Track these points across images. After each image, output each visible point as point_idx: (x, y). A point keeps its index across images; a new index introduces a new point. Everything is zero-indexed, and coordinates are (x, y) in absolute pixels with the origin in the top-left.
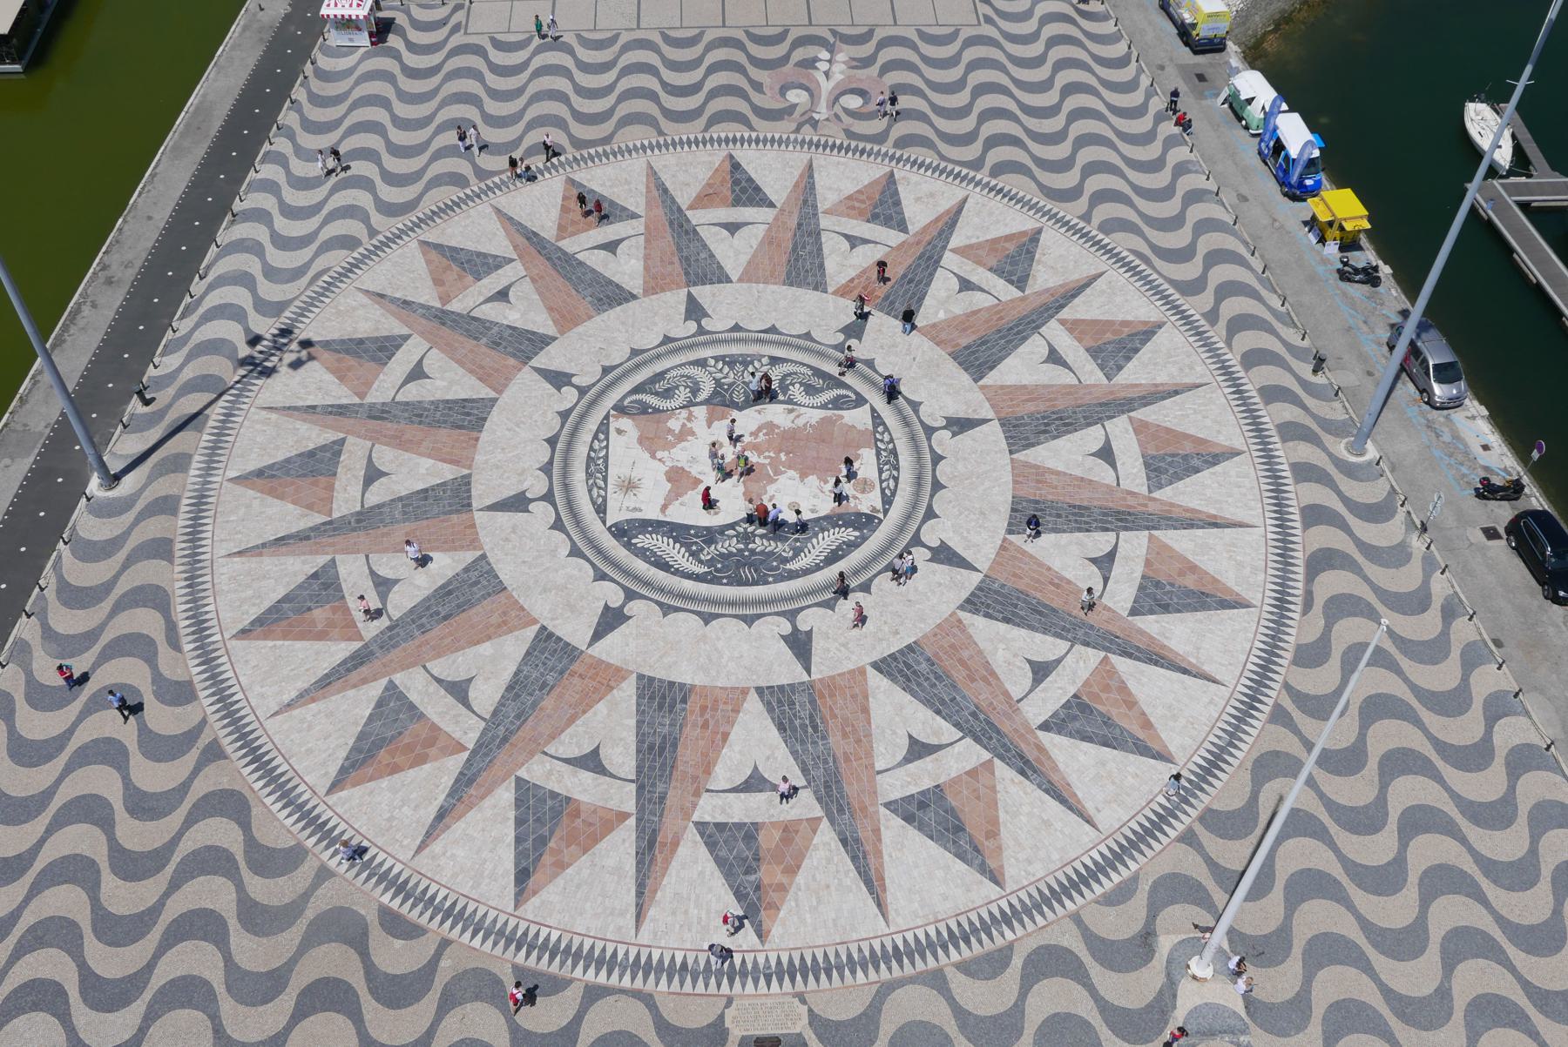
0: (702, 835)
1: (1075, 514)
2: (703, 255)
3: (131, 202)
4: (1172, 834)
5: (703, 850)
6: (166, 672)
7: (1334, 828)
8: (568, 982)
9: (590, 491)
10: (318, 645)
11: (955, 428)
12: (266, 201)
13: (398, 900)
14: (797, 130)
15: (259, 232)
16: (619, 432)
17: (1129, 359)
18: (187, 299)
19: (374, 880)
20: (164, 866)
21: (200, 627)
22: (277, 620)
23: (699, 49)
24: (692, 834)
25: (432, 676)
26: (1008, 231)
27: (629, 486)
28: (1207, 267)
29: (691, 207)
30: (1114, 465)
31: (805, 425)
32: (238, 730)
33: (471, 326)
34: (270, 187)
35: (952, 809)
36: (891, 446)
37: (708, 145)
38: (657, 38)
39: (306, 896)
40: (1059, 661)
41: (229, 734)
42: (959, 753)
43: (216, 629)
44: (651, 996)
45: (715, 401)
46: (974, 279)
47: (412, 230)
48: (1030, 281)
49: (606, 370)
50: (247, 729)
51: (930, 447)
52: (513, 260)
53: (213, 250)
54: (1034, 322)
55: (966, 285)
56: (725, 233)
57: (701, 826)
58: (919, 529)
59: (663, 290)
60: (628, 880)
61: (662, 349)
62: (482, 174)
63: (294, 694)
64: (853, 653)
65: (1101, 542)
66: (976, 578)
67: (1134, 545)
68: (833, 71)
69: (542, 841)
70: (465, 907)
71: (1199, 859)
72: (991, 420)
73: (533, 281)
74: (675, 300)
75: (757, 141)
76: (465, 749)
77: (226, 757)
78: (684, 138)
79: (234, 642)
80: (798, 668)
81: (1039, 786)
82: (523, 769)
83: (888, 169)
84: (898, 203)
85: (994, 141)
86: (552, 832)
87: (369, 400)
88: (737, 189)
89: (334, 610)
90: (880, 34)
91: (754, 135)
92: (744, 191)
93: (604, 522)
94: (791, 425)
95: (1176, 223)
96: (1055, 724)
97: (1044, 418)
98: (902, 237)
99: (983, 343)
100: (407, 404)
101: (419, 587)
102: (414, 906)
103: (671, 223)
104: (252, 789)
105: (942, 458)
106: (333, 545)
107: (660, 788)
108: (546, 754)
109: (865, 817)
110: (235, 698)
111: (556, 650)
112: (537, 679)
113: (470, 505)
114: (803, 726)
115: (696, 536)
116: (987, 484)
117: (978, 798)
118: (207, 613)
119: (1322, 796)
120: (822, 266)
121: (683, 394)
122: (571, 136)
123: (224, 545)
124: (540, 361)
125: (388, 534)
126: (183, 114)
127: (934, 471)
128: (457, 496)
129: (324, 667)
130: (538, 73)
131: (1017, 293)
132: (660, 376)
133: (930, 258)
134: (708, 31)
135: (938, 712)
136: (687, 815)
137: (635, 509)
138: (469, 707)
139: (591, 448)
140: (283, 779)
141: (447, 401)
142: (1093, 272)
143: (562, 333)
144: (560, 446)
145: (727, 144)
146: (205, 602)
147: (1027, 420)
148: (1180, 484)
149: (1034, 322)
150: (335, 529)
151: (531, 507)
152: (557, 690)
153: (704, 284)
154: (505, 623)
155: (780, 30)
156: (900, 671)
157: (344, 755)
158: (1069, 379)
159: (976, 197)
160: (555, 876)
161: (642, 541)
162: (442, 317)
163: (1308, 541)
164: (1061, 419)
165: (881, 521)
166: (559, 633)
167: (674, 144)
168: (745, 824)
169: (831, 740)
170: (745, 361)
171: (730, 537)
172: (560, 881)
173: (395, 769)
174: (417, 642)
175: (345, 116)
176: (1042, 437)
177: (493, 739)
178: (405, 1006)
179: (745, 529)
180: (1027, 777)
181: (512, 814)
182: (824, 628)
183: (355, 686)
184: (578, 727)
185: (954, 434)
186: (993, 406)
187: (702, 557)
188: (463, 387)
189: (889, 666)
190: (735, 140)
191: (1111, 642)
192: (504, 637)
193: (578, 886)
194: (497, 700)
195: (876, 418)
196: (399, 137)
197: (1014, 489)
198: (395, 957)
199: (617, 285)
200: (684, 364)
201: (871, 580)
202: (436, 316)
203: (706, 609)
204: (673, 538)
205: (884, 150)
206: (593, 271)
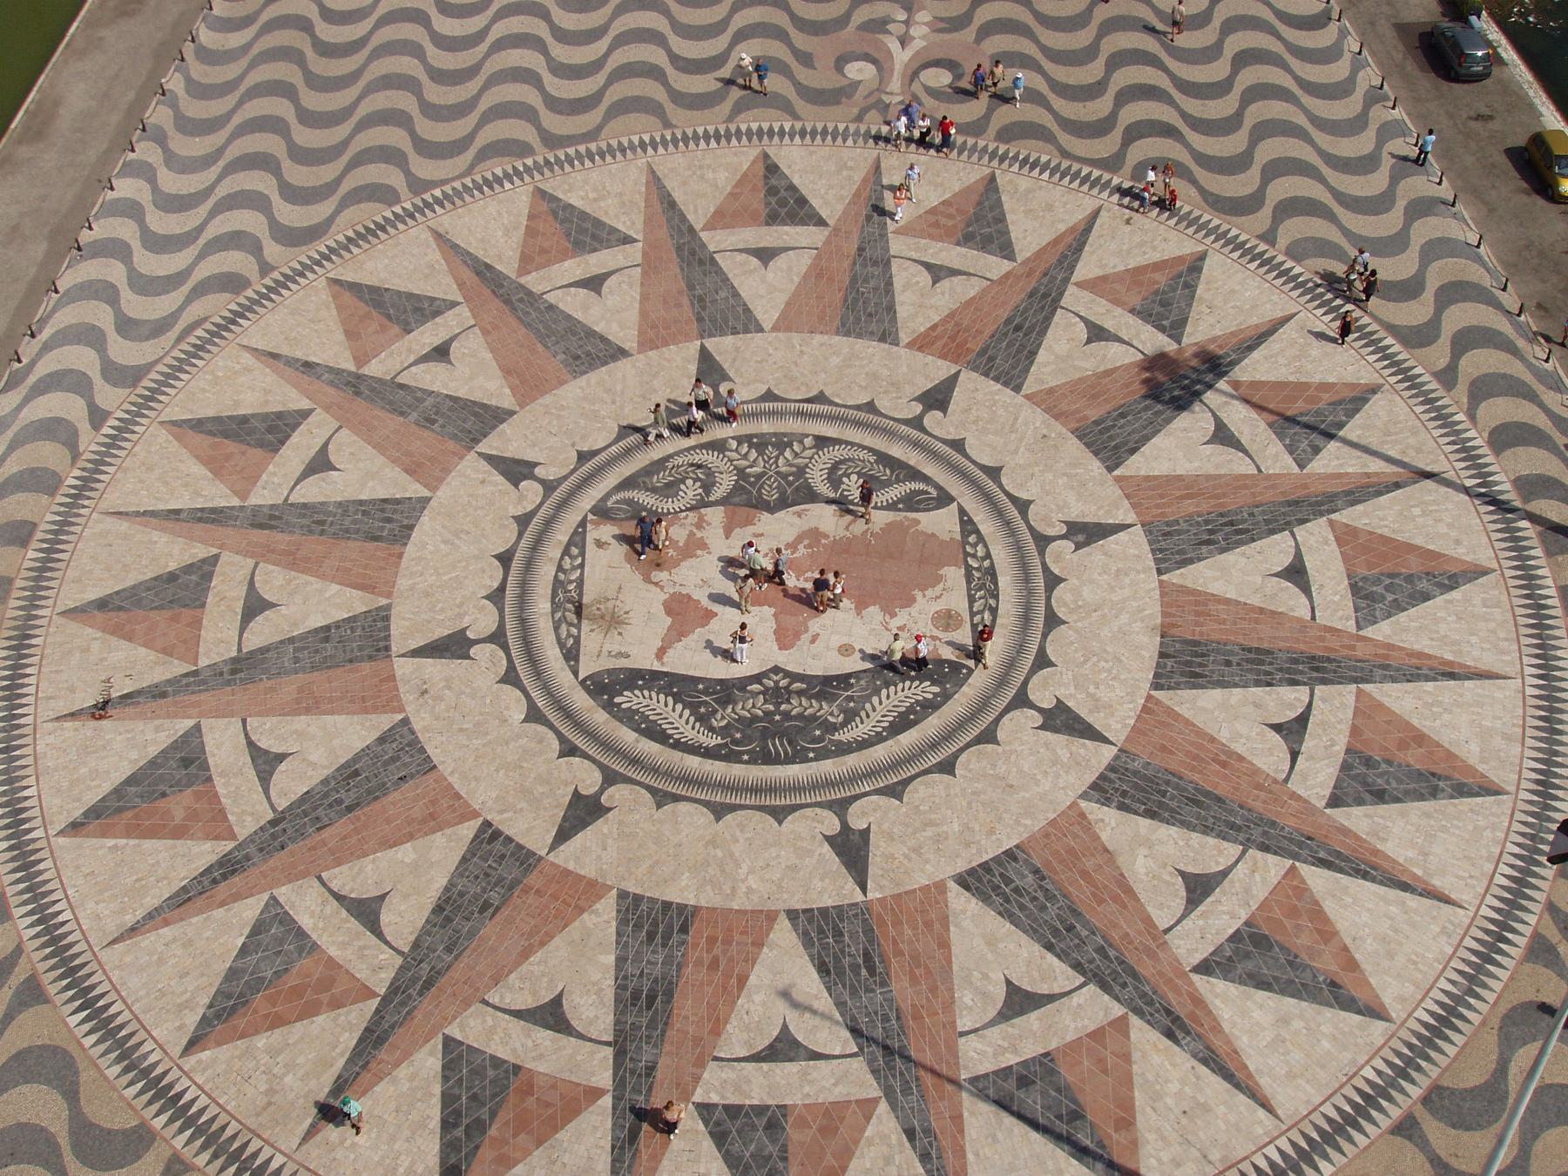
1: (1247, 661)
2: (723, 294)
4: (1385, 1123)
5: (708, 1144)
9: (556, 629)
11: (1081, 538)
12: (125, 230)
14: (859, 118)
15: (115, 272)
16: (600, 544)
22: (119, 810)
25: (331, 891)
26: (1156, 257)
28: (1440, 306)
29: (709, 226)
30: (1306, 589)
32: (63, 962)
34: (132, 210)
35: (1068, 1088)
36: (987, 563)
37: (734, 141)
40: (1225, 873)
45: (736, 500)
46: (1108, 324)
47: (319, 264)
48: (1188, 329)
49: (583, 457)
50: (77, 962)
51: (1044, 565)
52: (458, 304)
55: (1097, 334)
56: (754, 262)
57: (705, 1109)
59: (666, 344)
62: (418, 186)
63: (140, 914)
64: (927, 861)
65: (1287, 700)
66: (1107, 753)
69: (479, 1127)
71: (1421, 1158)
72: (1130, 526)
73: (485, 332)
75: (803, 133)
76: (374, 995)
77: (47, 1001)
78: (700, 131)
79: (61, 840)
80: (850, 885)
81: (1195, 1056)
83: (988, 171)
84: (1001, 219)
85: (1134, 133)
86: (493, 1115)
87: (254, 500)
88: (773, 200)
89: (198, 796)
91: (798, 125)
92: (783, 203)
96: (1218, 963)
97: (1207, 522)
98: (1006, 266)
99: (1122, 416)
100: (305, 506)
101: (313, 765)
103: (679, 248)
104: (81, 1045)
108: (487, 1004)
109: (941, 1098)
110: (61, 918)
112: (476, 897)
113: (387, 648)
114: (855, 968)
115: (705, 692)
116: (1124, 618)
117: (1105, 1071)
118: (26, 798)
120: (891, 309)
121: (691, 491)
123: (52, 703)
124: (489, 445)
125: (272, 689)
127: (1048, 599)
129: (182, 874)
130: (499, 45)
132: (660, 464)
133: (1045, 296)
135: (1049, 947)
137: (620, 655)
138: (379, 935)
139: (560, 568)
140: (123, 1033)
141: (361, 503)
142: (1279, 314)
143: (522, 406)
144: (517, 564)
145: (760, 139)
147: (1184, 526)
148: (1402, 617)
150: (203, 682)
151: (472, 652)
154: (432, 816)
156: (996, 888)
157: (207, 1001)
158: (1243, 466)
161: (627, 700)
162: (355, 384)
164: (1231, 523)
165: (971, 671)
166: (508, 832)
167: (685, 139)
168: (768, 1107)
169: (894, 986)
170: (782, 442)
171: (755, 694)
173: (277, 1022)
174: (308, 842)
175: (233, 111)
176: (1204, 549)
177: (414, 980)
179: (776, 683)
180: (1176, 1041)
181: (437, 1089)
182: (885, 826)
183: (222, 904)
184: (534, 963)
185: (1078, 547)
186: (1134, 506)
187: (715, 723)
188: (387, 481)
189: (980, 880)
191: (1300, 845)
192: (433, 837)
195: (968, 525)
196: (305, 137)
199: (603, 339)
200: (693, 448)
201: (956, 756)
202: (348, 384)
204: (674, 695)
205: (981, 144)
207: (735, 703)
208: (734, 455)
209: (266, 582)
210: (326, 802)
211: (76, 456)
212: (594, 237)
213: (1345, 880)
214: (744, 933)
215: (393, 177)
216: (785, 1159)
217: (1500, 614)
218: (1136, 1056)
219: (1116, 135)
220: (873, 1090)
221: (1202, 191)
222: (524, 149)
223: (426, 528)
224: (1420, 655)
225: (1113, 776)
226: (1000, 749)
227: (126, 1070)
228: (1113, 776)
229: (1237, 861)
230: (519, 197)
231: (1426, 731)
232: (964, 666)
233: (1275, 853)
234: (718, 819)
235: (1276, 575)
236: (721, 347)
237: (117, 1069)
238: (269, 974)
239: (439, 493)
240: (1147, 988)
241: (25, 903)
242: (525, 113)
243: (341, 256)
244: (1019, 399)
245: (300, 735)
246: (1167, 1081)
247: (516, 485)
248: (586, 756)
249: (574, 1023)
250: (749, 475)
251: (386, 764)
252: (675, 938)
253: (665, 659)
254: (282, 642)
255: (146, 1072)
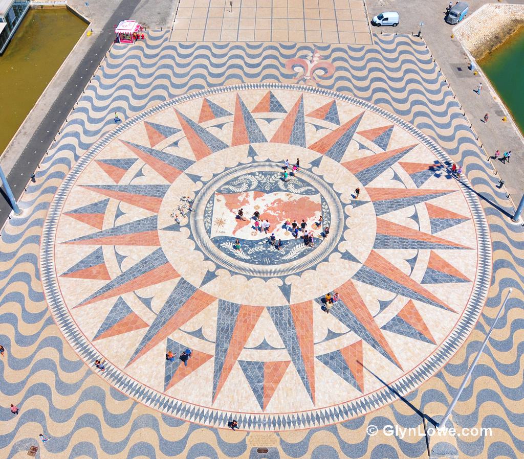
0: (241, 366)
1: (402, 242)
3: (36, 104)
5: (241, 372)
6: (34, 289)
7: (498, 373)
8: (185, 421)
9: (205, 224)
10: (95, 281)
11: (355, 205)
12: (87, 105)
13: (118, 385)
14: (298, 83)
16: (218, 200)
17: (426, 179)
18: (53, 142)
19: (109, 376)
20: (28, 365)
21: (48, 270)
23: (260, 50)
24: (237, 366)
26: (380, 126)
27: (221, 222)
28: (459, 144)
29: (254, 111)
30: (418, 222)
31: (294, 201)
32: (60, 313)
33: (161, 155)
34: (89, 99)
36: (328, 211)
37: (262, 88)
38: (245, 47)
39: (82, 381)
40: (391, 301)
41: (57, 314)
42: (349, 337)
43: (54, 273)
44: (216, 429)
46: (366, 145)
47: (142, 117)
48: (388, 146)
49: (215, 176)
53: (65, 123)
54: (389, 163)
55: (362, 147)
57: (241, 362)
58: (337, 245)
59: (240, 144)
60: (210, 382)
61: (237, 168)
62: (171, 96)
65: (411, 253)
66: (359, 266)
67: (424, 256)
68: (314, 60)
70: (144, 390)
71: (443, 384)
73: (188, 138)
74: (245, 148)
75: (281, 87)
76: (148, 326)
78: (252, 84)
79: (60, 278)
80: (285, 300)
81: (380, 352)
82: (171, 335)
84: (336, 113)
85: (376, 90)
87: (120, 184)
88: (272, 105)
89: (100, 267)
90: (332, 47)
91: (280, 85)
92: (275, 106)
93: (210, 237)
94: (288, 200)
95: (447, 126)
97: (390, 202)
98: (337, 126)
99: (368, 171)
101: (133, 260)
102: (124, 387)
103: (245, 117)
105: (348, 216)
106: (101, 241)
107: (225, 345)
108: (180, 330)
110: (59, 300)
111: (187, 288)
113: (156, 227)
114: (285, 324)
115: (246, 244)
116: (366, 228)
119: (494, 359)
120: (304, 137)
121: (245, 187)
122: (207, 82)
126: (59, 70)
127: (345, 221)
128: (152, 224)
129: (96, 289)
130: (196, 57)
131: (384, 151)
133: (348, 136)
134: (265, 43)
135: (341, 320)
136: (236, 358)
137: (222, 232)
138: (150, 309)
139: (206, 207)
140: (76, 334)
141: (151, 186)
142: (414, 144)
146: (51, 261)
148: (444, 231)
149: (389, 163)
151: (180, 229)
152: (186, 304)
153: (256, 142)
154: (167, 276)
155: (293, 43)
159: (368, 112)
160: (181, 379)
161: (224, 245)
162: (151, 151)
163: (494, 256)
165: (322, 241)
166: (188, 281)
167: (248, 86)
172: (182, 382)
173: (120, 332)
176: (390, 209)
177: (160, 322)
178: (119, 427)
180: (375, 348)
182: (296, 284)
183: (106, 298)
185: (354, 207)
186: (370, 196)
187: (248, 253)
188: (160, 180)
190: (272, 86)
191: (413, 294)
193: (190, 384)
194: (162, 307)
195: (323, 199)
196: (140, 81)
197: (377, 230)
198: (116, 407)
199: (222, 142)
201: (317, 265)
203: (249, 274)
206: (212, 135)
207: (255, 247)
208: (257, 177)
209: (122, 207)
210: (137, 270)
211: (70, 169)
212: (221, 113)
213: (425, 304)
214: (254, 313)
215: (164, 93)
216: (263, 377)
217: (472, 232)
218: (364, 352)
219: (370, 91)
220: (289, 359)
221: (393, 108)
222: (202, 87)
223: (169, 193)
224: (449, 242)
225: (361, 273)
226: (330, 263)
227: (76, 344)
228: (361, 273)
229: (395, 298)
230: (199, 101)
231: (450, 263)
232: (320, 240)
233: (406, 296)
234: (248, 279)
235: (410, 217)
236: (255, 146)
237: (74, 344)
238: (118, 319)
239: (173, 184)
240: (368, 333)
241: (49, 295)
242: (203, 77)
243: (148, 115)
244: (339, 164)
245: (131, 251)
246: (372, 359)
247: (195, 183)
248: (212, 261)
249: (204, 336)
250: (262, 183)
251: (154, 260)
252: (235, 313)
253: (235, 234)
254: (126, 224)
255: (82, 345)
